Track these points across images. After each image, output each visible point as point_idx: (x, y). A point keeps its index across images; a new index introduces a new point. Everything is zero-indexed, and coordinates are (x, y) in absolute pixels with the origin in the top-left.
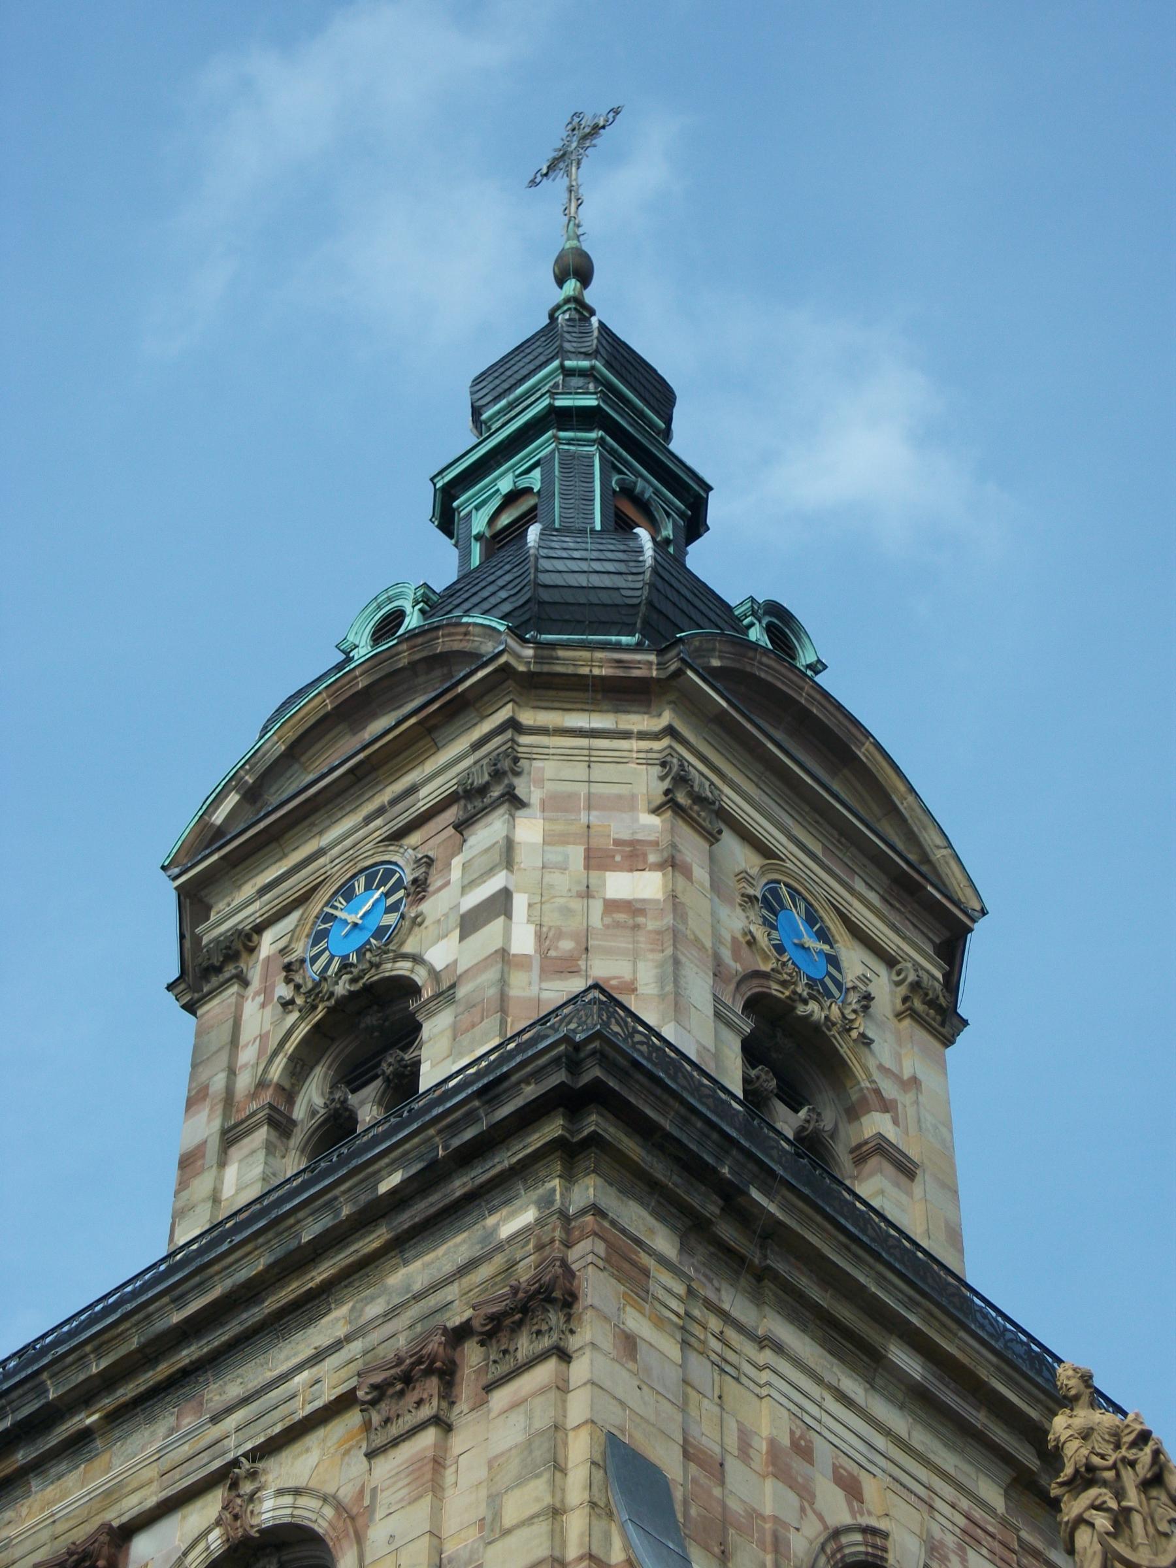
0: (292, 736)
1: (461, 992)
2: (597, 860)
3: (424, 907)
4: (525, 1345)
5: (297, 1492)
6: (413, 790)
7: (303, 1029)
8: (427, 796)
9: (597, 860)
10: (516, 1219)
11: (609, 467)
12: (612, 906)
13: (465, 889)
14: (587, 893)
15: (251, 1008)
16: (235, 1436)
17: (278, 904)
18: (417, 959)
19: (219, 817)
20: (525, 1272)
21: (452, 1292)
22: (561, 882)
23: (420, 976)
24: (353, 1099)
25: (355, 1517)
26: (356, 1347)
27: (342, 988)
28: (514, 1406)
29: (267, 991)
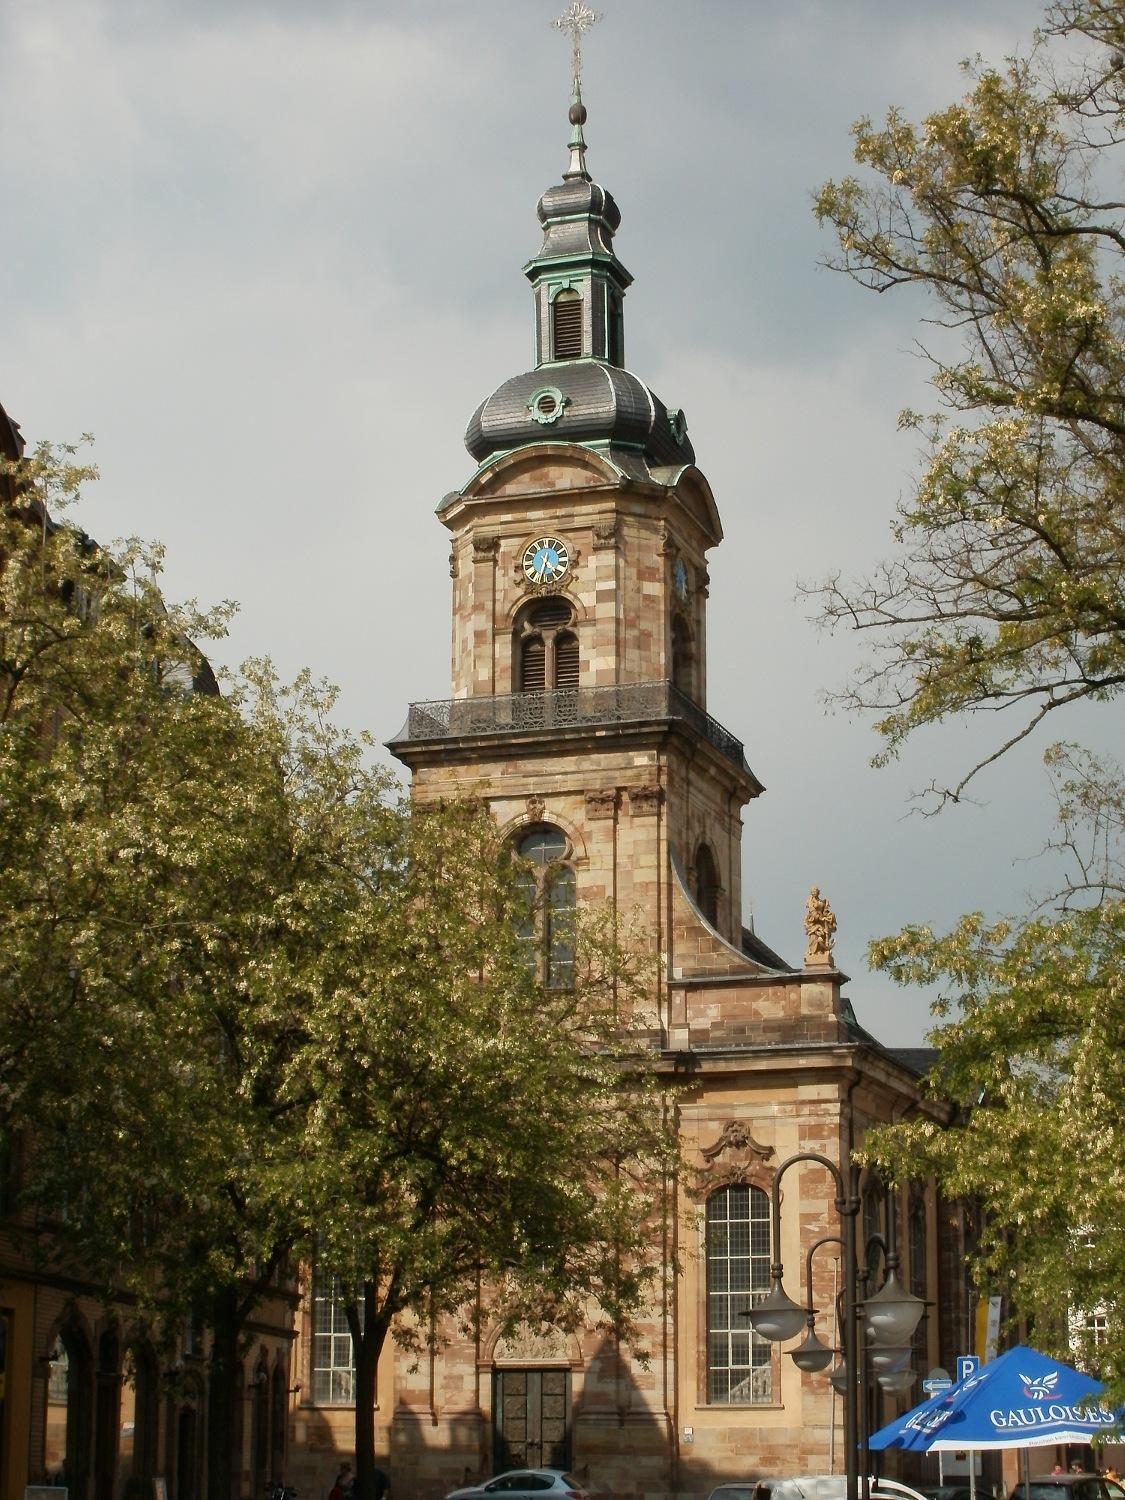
0: (518, 458)
1: (599, 627)
2: (641, 576)
3: (575, 572)
4: (646, 807)
5: (559, 816)
6: (572, 516)
7: (525, 600)
8: (578, 522)
9: (641, 576)
10: (641, 759)
11: (609, 288)
12: (647, 597)
13: (599, 579)
14: (639, 590)
15: (499, 573)
16: (532, 786)
17: (509, 532)
18: (576, 596)
19: (484, 480)
20: (644, 781)
21: (617, 774)
22: (631, 584)
23: (577, 605)
24: (545, 634)
25: (584, 837)
26: (581, 776)
27: (543, 591)
28: (643, 826)
29: (505, 569)
